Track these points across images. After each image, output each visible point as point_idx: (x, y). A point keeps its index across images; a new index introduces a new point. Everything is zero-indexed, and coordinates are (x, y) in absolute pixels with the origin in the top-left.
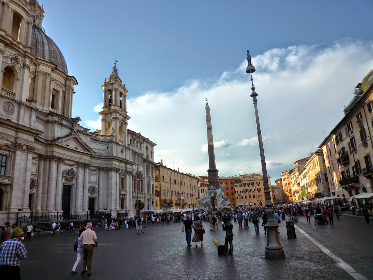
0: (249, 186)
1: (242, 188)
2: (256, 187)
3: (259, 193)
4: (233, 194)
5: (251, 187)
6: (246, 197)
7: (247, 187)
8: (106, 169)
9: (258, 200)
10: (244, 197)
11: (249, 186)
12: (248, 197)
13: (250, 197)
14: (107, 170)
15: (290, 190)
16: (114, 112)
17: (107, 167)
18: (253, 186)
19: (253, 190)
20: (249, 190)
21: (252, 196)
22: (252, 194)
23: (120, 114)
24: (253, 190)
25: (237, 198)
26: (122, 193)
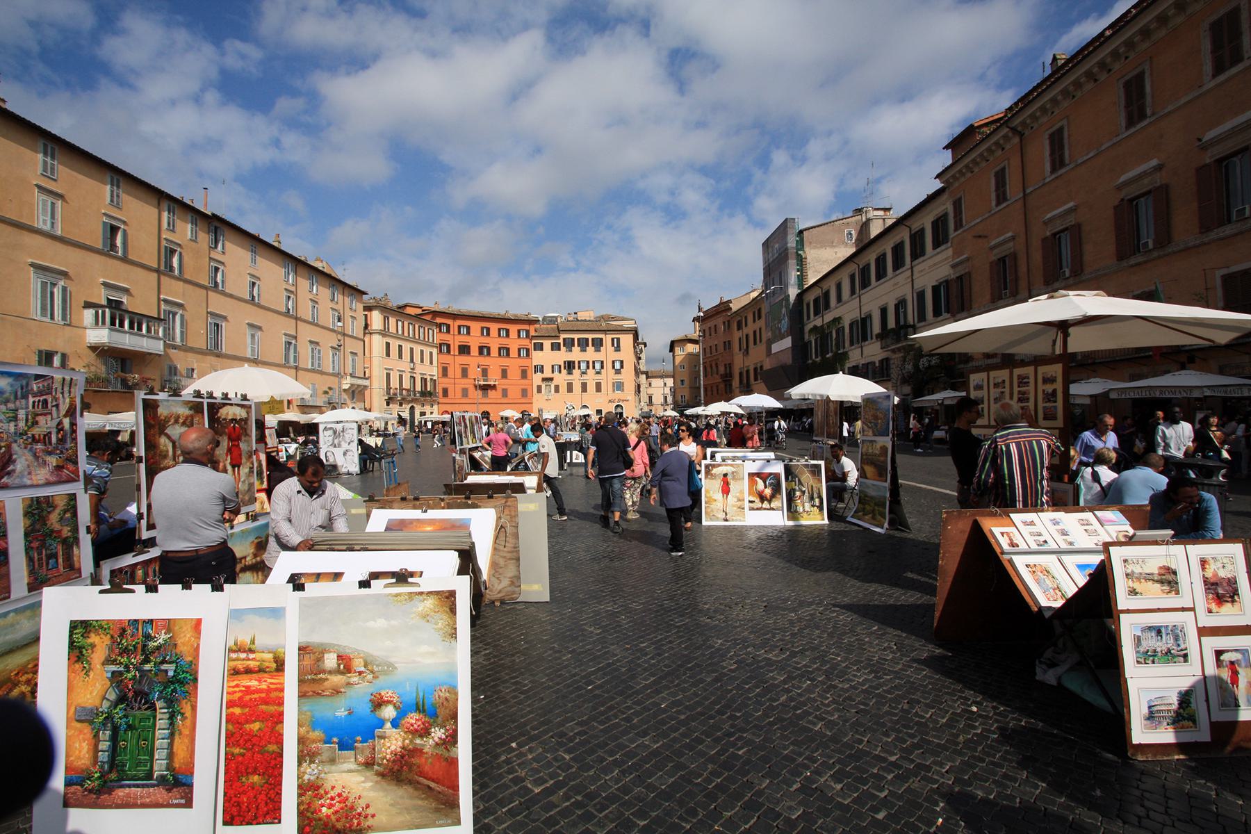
0: (583, 350)
1: (562, 356)
3: (618, 376)
4: (524, 374)
5: (591, 354)
6: (570, 388)
7: (576, 354)
10: (563, 388)
11: (583, 350)
12: (577, 387)
13: (584, 388)
15: (730, 366)
18: (598, 350)
19: (598, 366)
20: (583, 366)
21: (591, 387)
22: (591, 378)
24: (598, 366)
25: (539, 390)
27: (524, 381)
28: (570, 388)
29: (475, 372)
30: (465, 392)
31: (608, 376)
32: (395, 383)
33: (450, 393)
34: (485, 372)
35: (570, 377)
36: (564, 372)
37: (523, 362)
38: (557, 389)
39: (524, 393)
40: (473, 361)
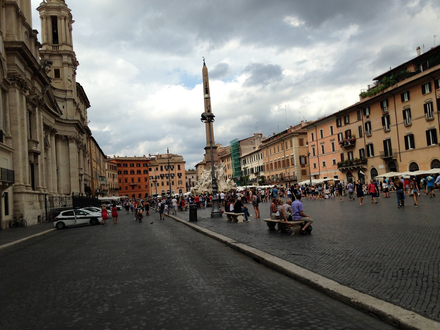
2: (176, 171)
6: (163, 184)
8: (64, 138)
9: (178, 188)
10: (160, 184)
12: (165, 184)
14: (67, 140)
16: (65, 54)
17: (66, 136)
20: (167, 176)
23: (72, 59)
25: (152, 185)
26: (81, 173)
27: (146, 183)
28: (163, 184)
29: (129, 181)
30: (126, 188)
31: (176, 179)
32: (110, 187)
33: (122, 188)
34: (133, 180)
35: (163, 180)
36: (160, 178)
37: (146, 176)
38: (158, 185)
39: (146, 187)
40: (129, 177)
